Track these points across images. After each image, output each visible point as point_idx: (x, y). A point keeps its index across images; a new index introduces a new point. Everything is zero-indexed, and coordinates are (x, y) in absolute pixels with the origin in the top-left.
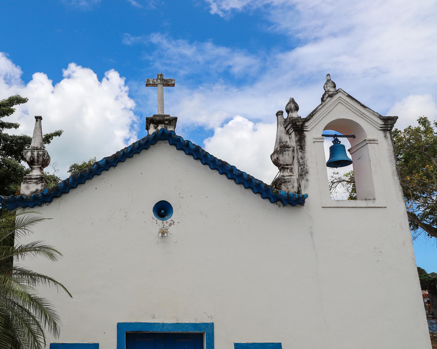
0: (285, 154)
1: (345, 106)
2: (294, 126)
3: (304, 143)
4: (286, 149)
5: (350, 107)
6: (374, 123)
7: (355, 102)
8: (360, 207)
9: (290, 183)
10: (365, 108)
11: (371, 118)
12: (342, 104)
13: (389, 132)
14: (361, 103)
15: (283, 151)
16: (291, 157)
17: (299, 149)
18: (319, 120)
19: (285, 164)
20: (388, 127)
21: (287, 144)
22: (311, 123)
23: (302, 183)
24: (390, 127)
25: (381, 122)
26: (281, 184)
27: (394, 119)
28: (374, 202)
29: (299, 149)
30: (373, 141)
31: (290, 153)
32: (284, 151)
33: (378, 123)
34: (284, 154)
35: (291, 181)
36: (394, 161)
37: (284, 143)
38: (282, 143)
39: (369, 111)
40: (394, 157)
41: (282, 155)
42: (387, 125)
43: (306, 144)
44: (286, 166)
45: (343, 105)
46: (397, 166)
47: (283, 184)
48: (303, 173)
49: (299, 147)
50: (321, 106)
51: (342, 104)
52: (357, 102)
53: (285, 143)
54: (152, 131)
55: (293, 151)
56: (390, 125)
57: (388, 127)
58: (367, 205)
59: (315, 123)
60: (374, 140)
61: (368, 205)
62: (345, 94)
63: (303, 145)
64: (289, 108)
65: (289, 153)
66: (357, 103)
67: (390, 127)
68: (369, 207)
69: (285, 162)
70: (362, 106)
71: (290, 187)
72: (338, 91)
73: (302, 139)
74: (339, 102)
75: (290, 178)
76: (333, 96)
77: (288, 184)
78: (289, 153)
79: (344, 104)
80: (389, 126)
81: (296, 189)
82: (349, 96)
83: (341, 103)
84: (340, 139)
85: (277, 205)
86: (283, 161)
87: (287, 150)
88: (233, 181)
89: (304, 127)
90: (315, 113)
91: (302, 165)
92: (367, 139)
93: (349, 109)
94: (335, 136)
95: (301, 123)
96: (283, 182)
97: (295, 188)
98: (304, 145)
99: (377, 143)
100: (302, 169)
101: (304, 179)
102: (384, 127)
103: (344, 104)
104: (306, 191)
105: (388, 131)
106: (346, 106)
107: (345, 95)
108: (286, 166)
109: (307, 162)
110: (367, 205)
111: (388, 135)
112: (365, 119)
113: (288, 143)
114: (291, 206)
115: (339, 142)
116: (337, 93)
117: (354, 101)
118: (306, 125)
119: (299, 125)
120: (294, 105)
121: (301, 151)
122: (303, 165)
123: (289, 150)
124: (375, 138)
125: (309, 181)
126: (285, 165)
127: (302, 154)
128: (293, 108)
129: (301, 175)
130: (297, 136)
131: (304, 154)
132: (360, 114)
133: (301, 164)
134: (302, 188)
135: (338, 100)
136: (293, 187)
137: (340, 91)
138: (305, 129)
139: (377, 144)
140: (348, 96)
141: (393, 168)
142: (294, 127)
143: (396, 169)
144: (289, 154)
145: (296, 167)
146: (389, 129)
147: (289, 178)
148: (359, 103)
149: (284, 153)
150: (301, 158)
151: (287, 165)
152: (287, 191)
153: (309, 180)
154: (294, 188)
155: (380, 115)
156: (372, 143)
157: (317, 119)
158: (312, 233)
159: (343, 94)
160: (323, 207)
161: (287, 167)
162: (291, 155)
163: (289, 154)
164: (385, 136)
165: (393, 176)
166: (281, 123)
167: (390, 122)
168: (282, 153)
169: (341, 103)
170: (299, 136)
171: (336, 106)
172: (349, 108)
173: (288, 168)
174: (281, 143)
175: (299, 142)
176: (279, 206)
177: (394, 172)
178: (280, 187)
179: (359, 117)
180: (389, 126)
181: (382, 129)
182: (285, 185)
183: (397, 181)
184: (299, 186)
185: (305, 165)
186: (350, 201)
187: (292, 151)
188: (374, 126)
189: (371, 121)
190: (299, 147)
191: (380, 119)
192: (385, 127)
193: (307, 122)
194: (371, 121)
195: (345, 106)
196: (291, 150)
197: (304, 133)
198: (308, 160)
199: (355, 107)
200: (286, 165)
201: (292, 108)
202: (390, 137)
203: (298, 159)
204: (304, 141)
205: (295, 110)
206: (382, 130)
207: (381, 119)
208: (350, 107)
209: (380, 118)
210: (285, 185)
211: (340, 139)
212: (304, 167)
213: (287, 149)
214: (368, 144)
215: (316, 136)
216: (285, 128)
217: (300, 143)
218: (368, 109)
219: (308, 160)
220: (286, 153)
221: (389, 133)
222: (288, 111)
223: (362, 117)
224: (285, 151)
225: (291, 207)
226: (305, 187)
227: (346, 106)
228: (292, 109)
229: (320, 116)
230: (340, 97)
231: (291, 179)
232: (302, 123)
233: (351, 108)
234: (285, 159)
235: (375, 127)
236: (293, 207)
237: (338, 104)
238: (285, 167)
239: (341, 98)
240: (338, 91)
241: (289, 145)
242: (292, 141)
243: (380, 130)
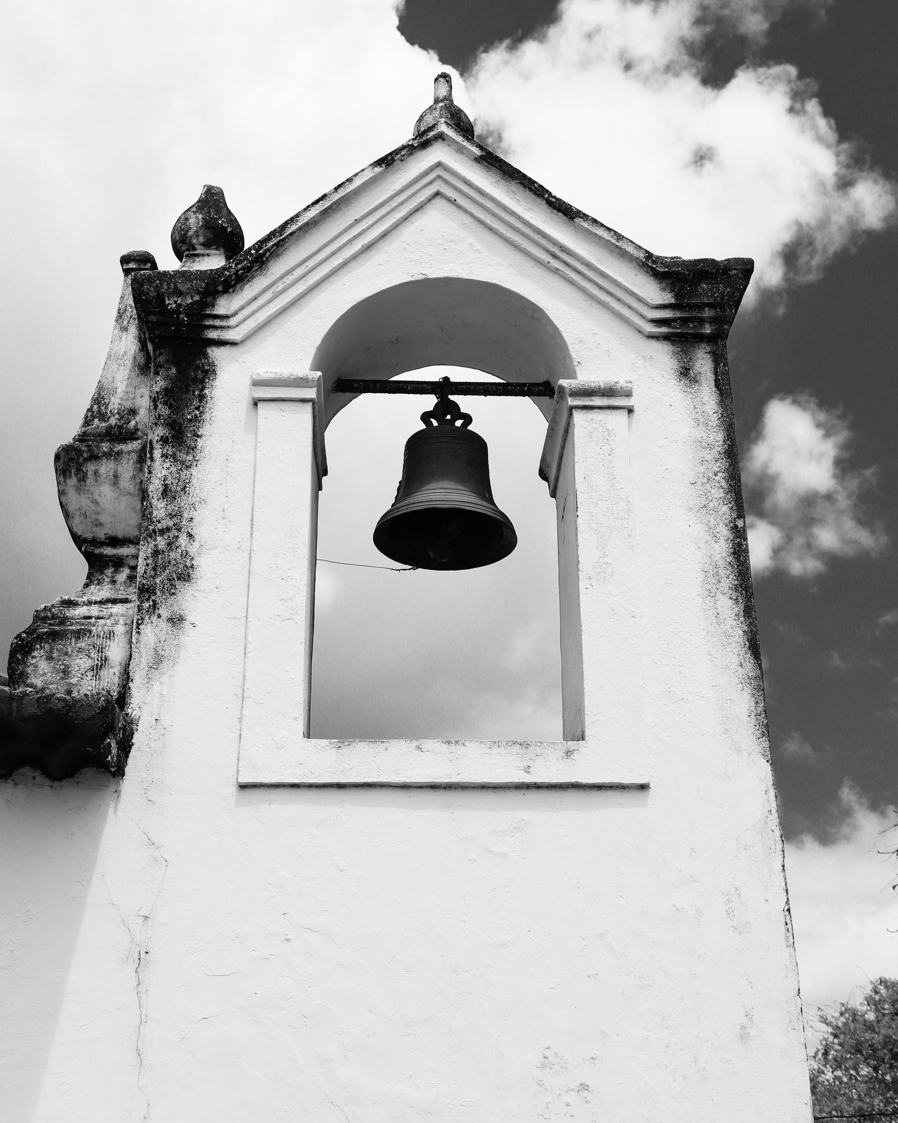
0: (96, 473)
1: (465, 211)
2: (150, 313)
3: (198, 408)
4: (98, 447)
5: (494, 215)
6: (619, 300)
7: (522, 188)
8: (484, 787)
9: (82, 644)
10: (572, 218)
11: (603, 275)
12: (453, 202)
13: (708, 349)
14: (550, 194)
15: (81, 460)
16: (129, 494)
17: (164, 440)
18: (302, 282)
19: (101, 534)
20: (701, 321)
21: (133, 423)
22: (255, 298)
23: (143, 638)
24: (713, 321)
27: (730, 277)
28: (568, 753)
29: (164, 440)
31: (127, 469)
32: (86, 460)
33: (639, 299)
34: (90, 473)
35: (94, 628)
36: (725, 509)
37: (113, 421)
38: (103, 417)
39: (592, 233)
40: (724, 484)
41: (79, 481)
42: (690, 307)
43: (207, 416)
44: (108, 551)
45: (459, 207)
46: (738, 537)
47: (41, 648)
48: (158, 580)
49: (160, 431)
50: (317, 206)
51: (453, 202)
52: (531, 190)
53: (122, 418)
56: (711, 306)
57: (701, 321)
58: (527, 770)
59: (277, 301)
60: (609, 392)
61: (531, 770)
62: (466, 148)
63: (190, 420)
64: (176, 234)
65: (120, 469)
66: (531, 196)
67: (713, 321)
68: (538, 787)
69: (100, 525)
70: (555, 208)
71: (80, 663)
72: (431, 134)
73: (187, 386)
74: (437, 194)
75: (101, 614)
76: (393, 160)
77: (72, 645)
78: (116, 472)
79: (461, 201)
80: (707, 313)
81: (110, 679)
83: (449, 200)
84: (465, 402)
86: (85, 516)
87: (108, 455)
89: (207, 323)
90: (277, 245)
91: (162, 532)
92: (565, 385)
93: (491, 229)
94: (443, 388)
95: (189, 301)
96: (40, 638)
97: (112, 671)
98: (197, 420)
99: (630, 411)
100: (156, 553)
101: (159, 616)
102: (674, 320)
103: (461, 201)
104: (157, 687)
105: (704, 345)
106: (471, 215)
107: (469, 154)
108: (108, 551)
109: (193, 514)
110: (527, 770)
111: (703, 363)
112: (572, 282)
113: (137, 419)
114: (47, 782)
115: (459, 423)
116: (425, 145)
117: (514, 186)
118: (220, 310)
119: (180, 313)
120: (200, 216)
121: (174, 456)
122: (168, 529)
123: (116, 450)
125: (186, 624)
126: (102, 544)
127: (173, 469)
128: (197, 234)
129: (148, 591)
130: (162, 372)
131: (188, 467)
132: (548, 251)
133: (159, 526)
135: (430, 183)
136: (97, 669)
137: (441, 137)
138: (213, 335)
139: (625, 412)
140: (481, 157)
141: (717, 547)
142: (152, 322)
143: (734, 553)
144: (116, 476)
146: (708, 329)
147: (94, 610)
148: (538, 191)
149: (91, 467)
150: (166, 491)
151: (114, 541)
153: (190, 618)
154: (104, 673)
155: (649, 256)
156: (600, 408)
157: (289, 279)
158: (142, 958)
159: (461, 150)
160: (243, 787)
161: (114, 556)
162: (126, 483)
163: (116, 476)
164: (685, 372)
166: (128, 314)
167: (711, 290)
168: (79, 471)
169: (449, 200)
170: (174, 370)
171: (420, 213)
172: (488, 220)
173: (118, 563)
174: (96, 420)
175: (165, 403)
177: (717, 574)
178: (18, 662)
179: (540, 272)
180: (707, 313)
181: (664, 330)
182: (51, 651)
183: (734, 623)
185: (179, 530)
186: (418, 748)
187: (134, 456)
188: (619, 316)
189: (601, 288)
190: (160, 431)
191: (652, 279)
192: (684, 321)
193: (225, 291)
194: (601, 288)
195: (465, 211)
196: (129, 453)
197: (206, 356)
198: (203, 501)
199: (519, 218)
200: (108, 545)
201: (190, 233)
202: (716, 373)
203: (144, 495)
204: (202, 397)
205: (207, 245)
206: (666, 338)
207: (657, 275)
208: (494, 215)
209: (653, 269)
210: (54, 655)
211: (465, 402)
212: (169, 544)
213: (105, 447)
215: (266, 371)
217: (170, 408)
218: (585, 225)
219: (203, 501)
220: (102, 470)
221: (708, 356)
223: (556, 271)
224: (94, 457)
225: (40, 786)
226: (158, 661)
227: (471, 215)
228: (191, 237)
229: (311, 263)
230: (439, 165)
231: (101, 622)
232: (197, 298)
233: (496, 225)
234: (97, 503)
235: (627, 322)
236: (56, 784)
237: (430, 200)
238: (101, 556)
239: (446, 169)
240: (431, 134)
241: (137, 430)
243: (652, 337)
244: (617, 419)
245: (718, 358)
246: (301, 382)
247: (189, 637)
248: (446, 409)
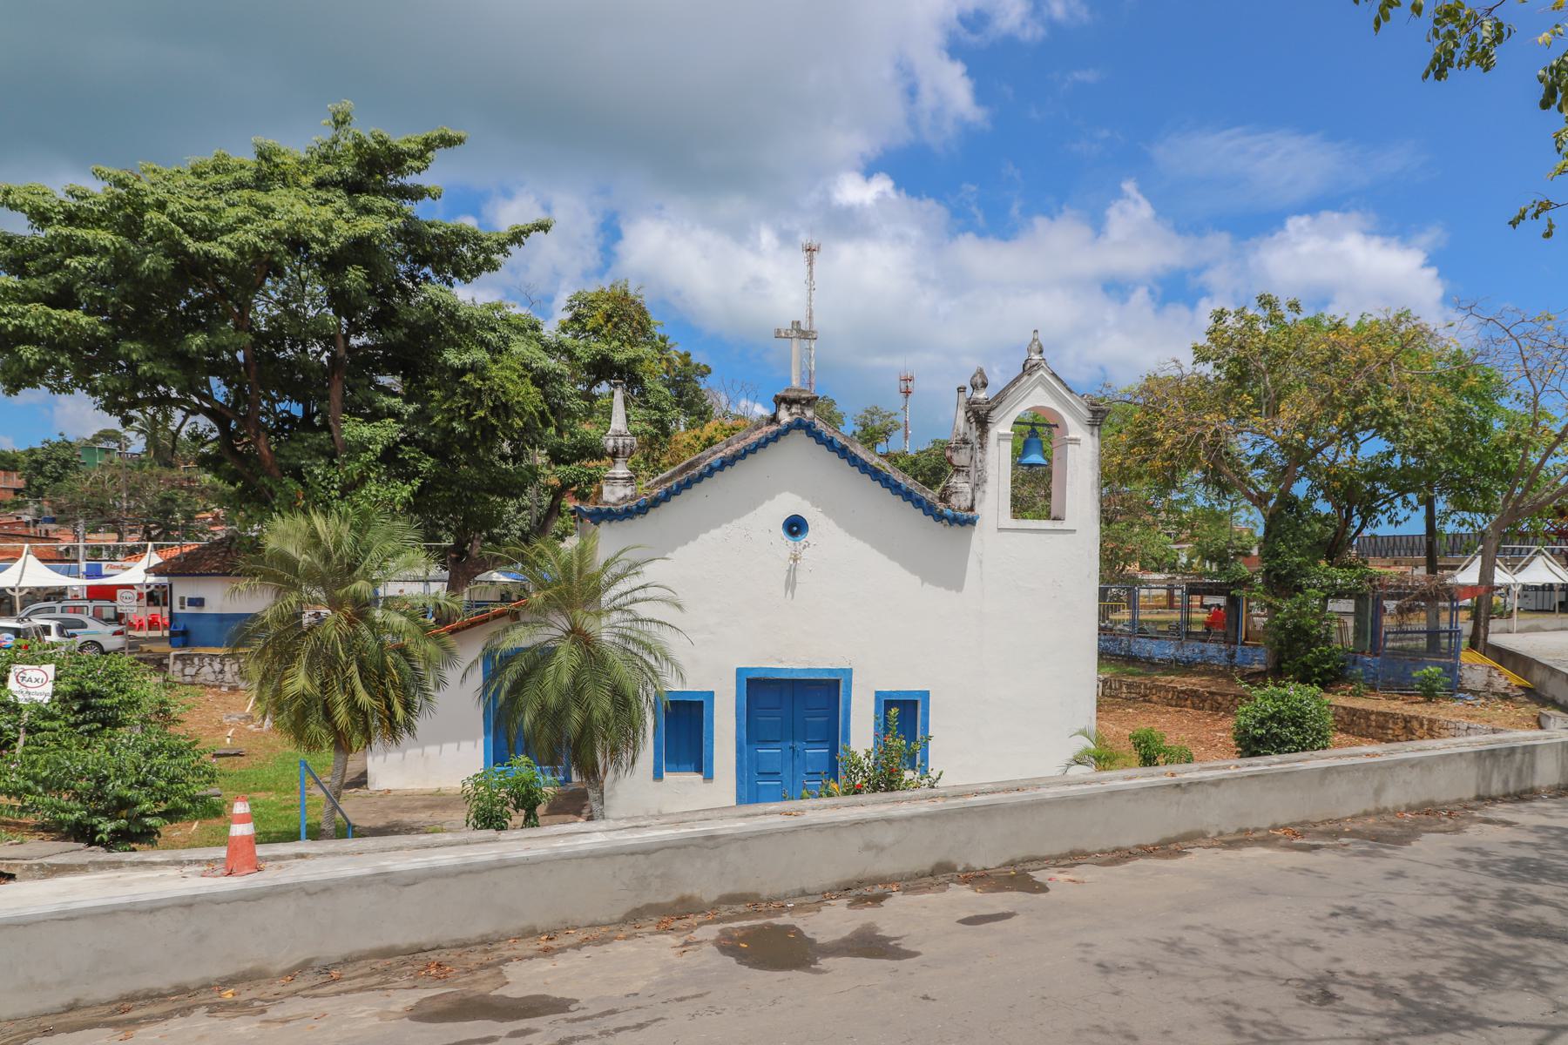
25: (1088, 415)
26: (950, 495)
30: (1076, 441)
31: (968, 451)
54: (785, 417)
55: (972, 449)
60: (1076, 440)
71: (962, 499)
82: (1054, 374)
85: (942, 525)
88: (888, 490)
124: (1078, 437)
134: (976, 502)
145: (972, 470)
152: (957, 505)
158: (981, 562)
160: (1000, 530)
164: (1092, 434)
165: (1092, 489)
176: (945, 525)
184: (973, 500)
214: (1069, 446)
216: (966, 413)
222: (974, 387)
226: (981, 501)
242: (973, 435)
244: (1077, 446)
245: (1099, 430)
246: (1009, 435)
247: (987, 496)
248: (1033, 431)
